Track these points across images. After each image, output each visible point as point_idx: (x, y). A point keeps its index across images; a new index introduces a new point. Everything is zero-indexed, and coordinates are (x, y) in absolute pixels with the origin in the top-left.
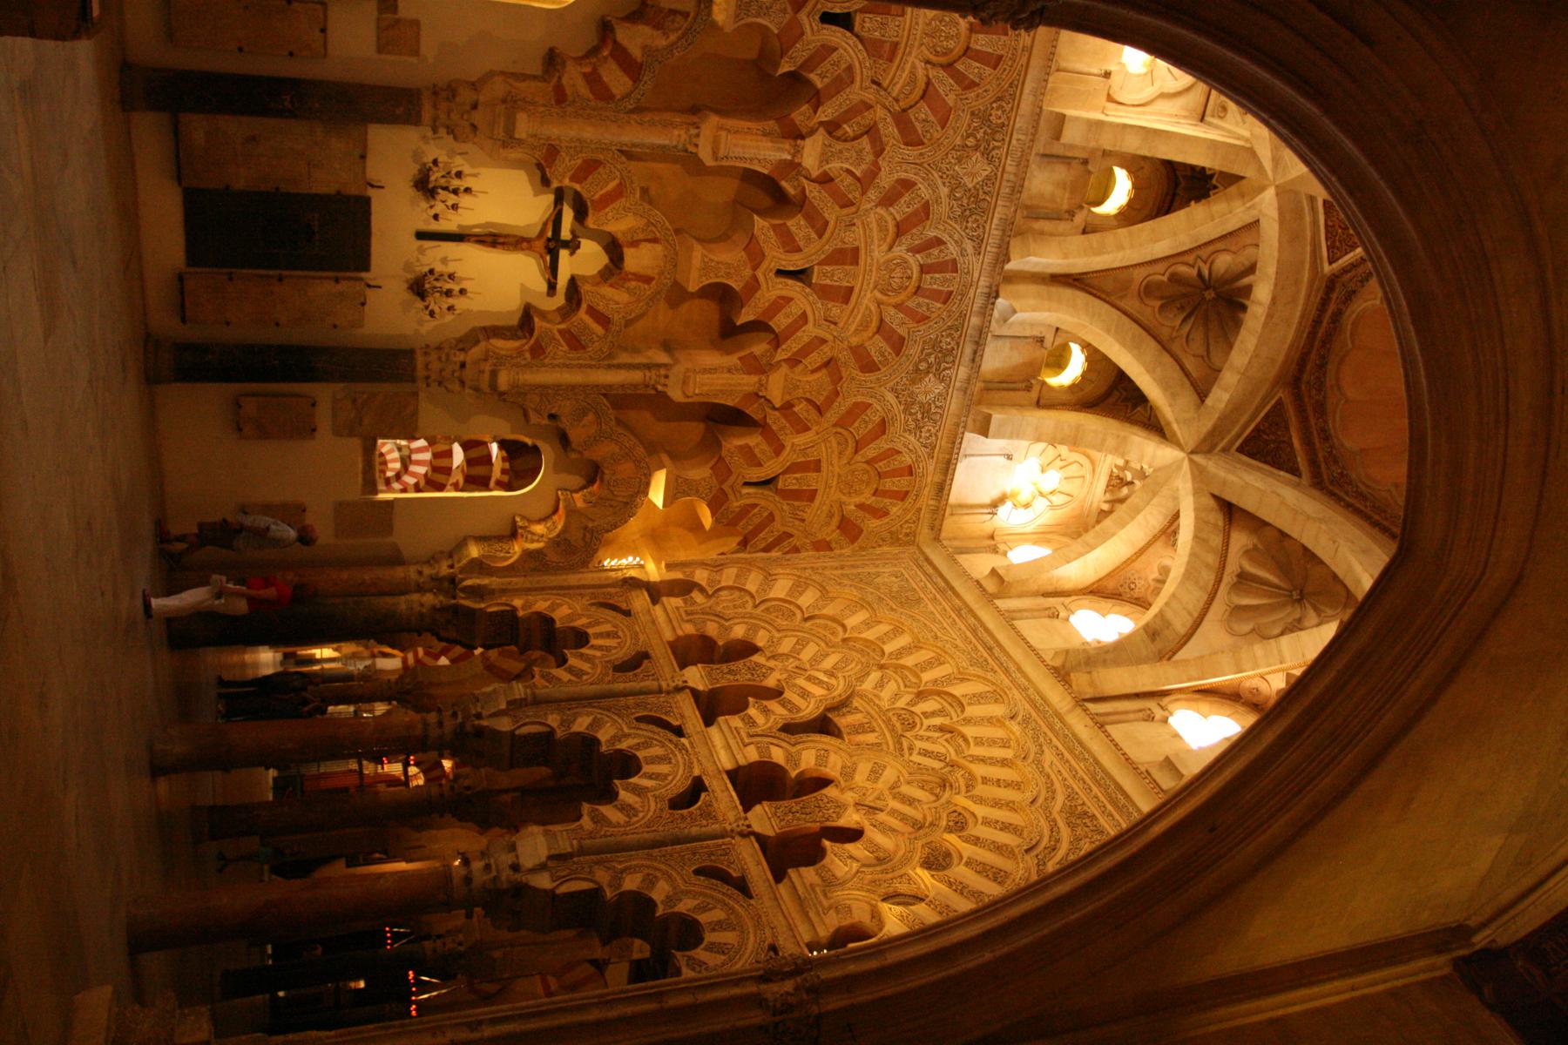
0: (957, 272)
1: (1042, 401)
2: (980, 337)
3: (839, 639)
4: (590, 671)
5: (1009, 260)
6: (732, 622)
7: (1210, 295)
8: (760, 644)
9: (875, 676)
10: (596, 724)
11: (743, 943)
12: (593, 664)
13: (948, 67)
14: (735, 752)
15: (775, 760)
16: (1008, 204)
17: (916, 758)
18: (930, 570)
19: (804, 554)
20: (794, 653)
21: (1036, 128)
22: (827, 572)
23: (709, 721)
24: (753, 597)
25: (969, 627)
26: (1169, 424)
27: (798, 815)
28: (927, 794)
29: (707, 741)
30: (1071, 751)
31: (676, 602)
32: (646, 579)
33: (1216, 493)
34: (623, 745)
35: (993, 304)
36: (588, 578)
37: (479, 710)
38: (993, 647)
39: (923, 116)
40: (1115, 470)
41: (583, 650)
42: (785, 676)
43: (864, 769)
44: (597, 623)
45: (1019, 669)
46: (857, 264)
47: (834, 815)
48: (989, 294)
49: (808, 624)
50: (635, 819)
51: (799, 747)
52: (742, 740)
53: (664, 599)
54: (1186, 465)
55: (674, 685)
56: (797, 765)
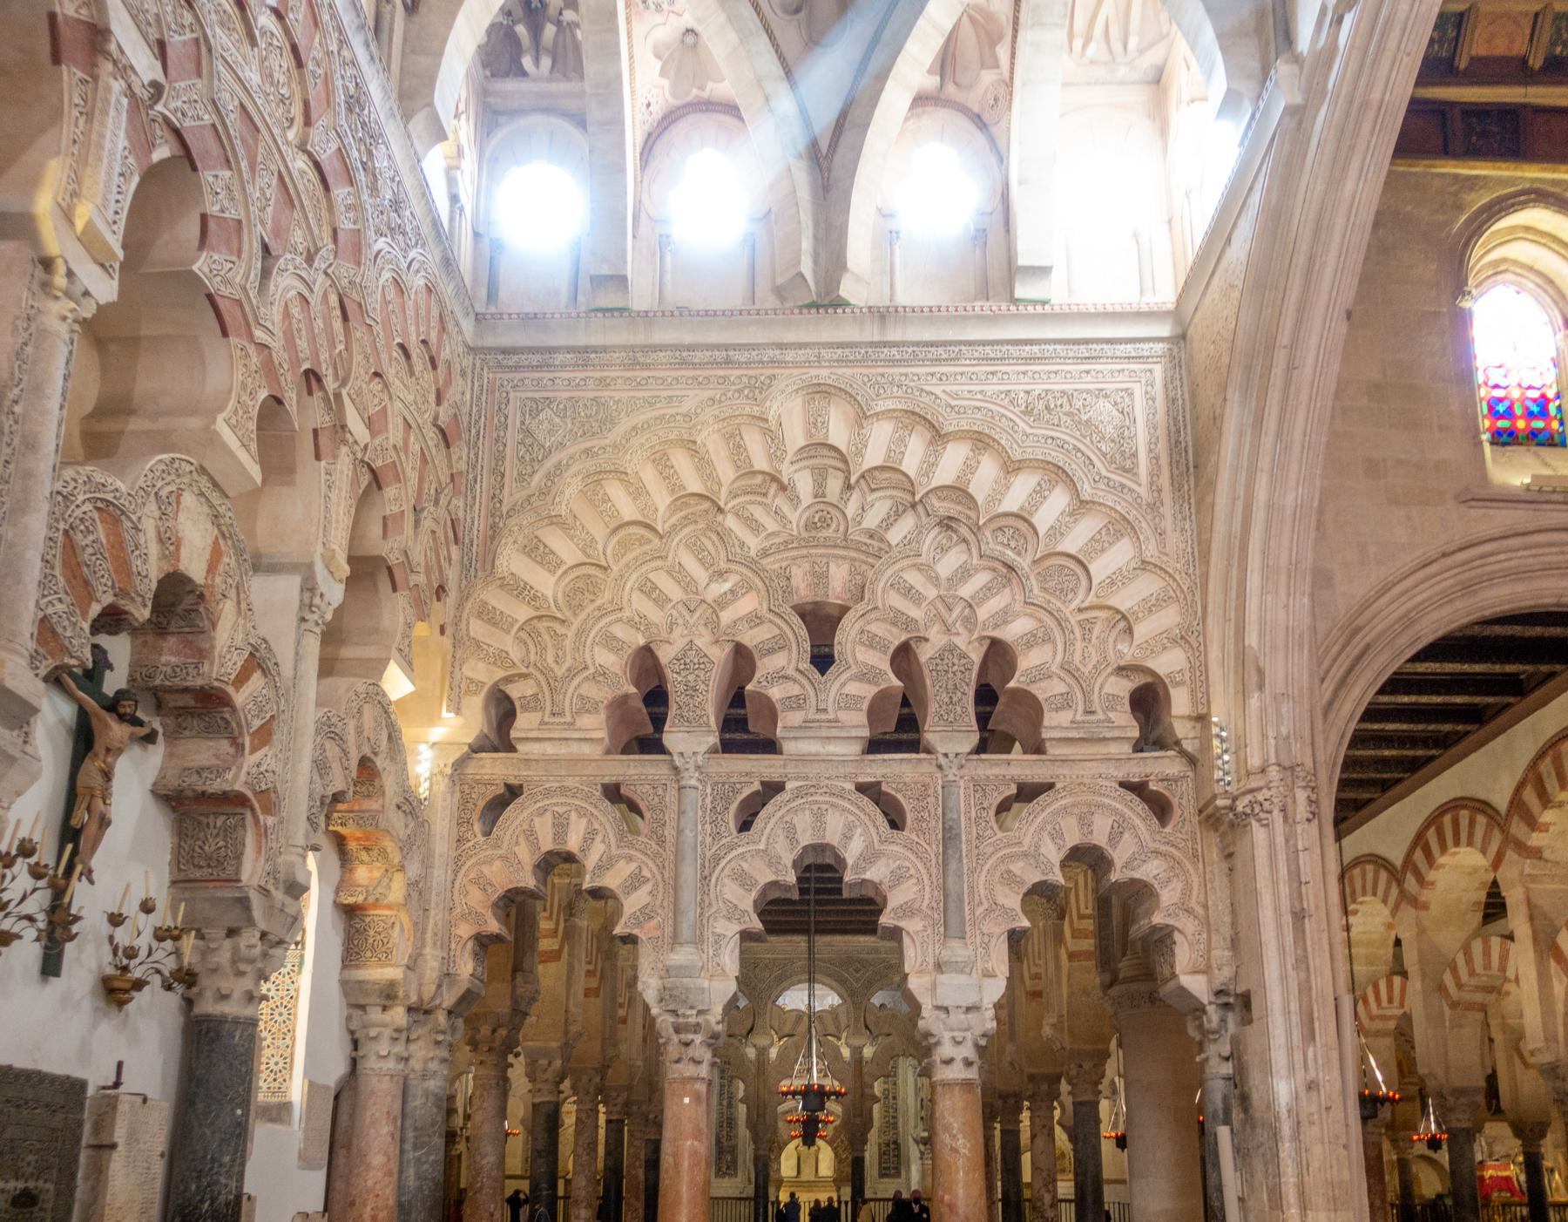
3: (656, 541)
4: (633, 866)
6: (589, 663)
8: (641, 641)
9: (731, 522)
10: (743, 879)
11: (1115, 811)
12: (620, 857)
14: (845, 734)
15: (870, 696)
17: (895, 536)
18: (535, 359)
19: (461, 514)
20: (661, 601)
22: (507, 501)
23: (769, 746)
24: (540, 618)
25: (672, 366)
27: (955, 699)
28: (954, 550)
29: (803, 759)
30: (938, 361)
31: (524, 723)
32: (466, 749)
34: (788, 858)
36: (442, 825)
37: (694, 1012)
38: (725, 356)
41: (591, 861)
42: (702, 629)
43: (897, 601)
44: (530, 834)
45: (780, 346)
47: (965, 661)
49: (615, 568)
50: (912, 871)
51: (851, 661)
52: (829, 721)
53: (514, 734)
55: (692, 769)
56: (882, 673)
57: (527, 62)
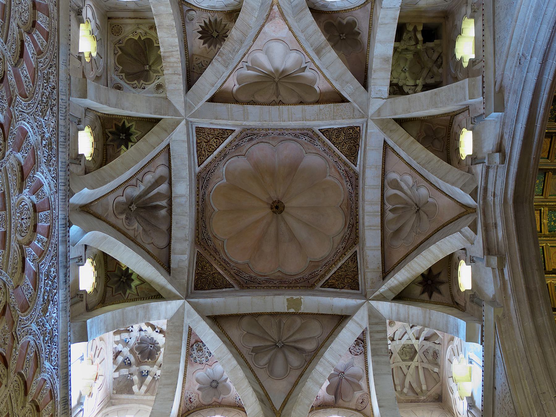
0: (50, 209)
1: (90, 306)
2: (66, 262)
5: (73, 194)
7: (134, 207)
13: (29, 33)
16: (64, 150)
21: (70, 90)
26: (163, 288)
33: (210, 314)
35: (69, 232)
39: (25, 72)
40: (115, 346)
46: (6, 210)
48: (66, 224)
54: (187, 306)
57: (135, 388)
